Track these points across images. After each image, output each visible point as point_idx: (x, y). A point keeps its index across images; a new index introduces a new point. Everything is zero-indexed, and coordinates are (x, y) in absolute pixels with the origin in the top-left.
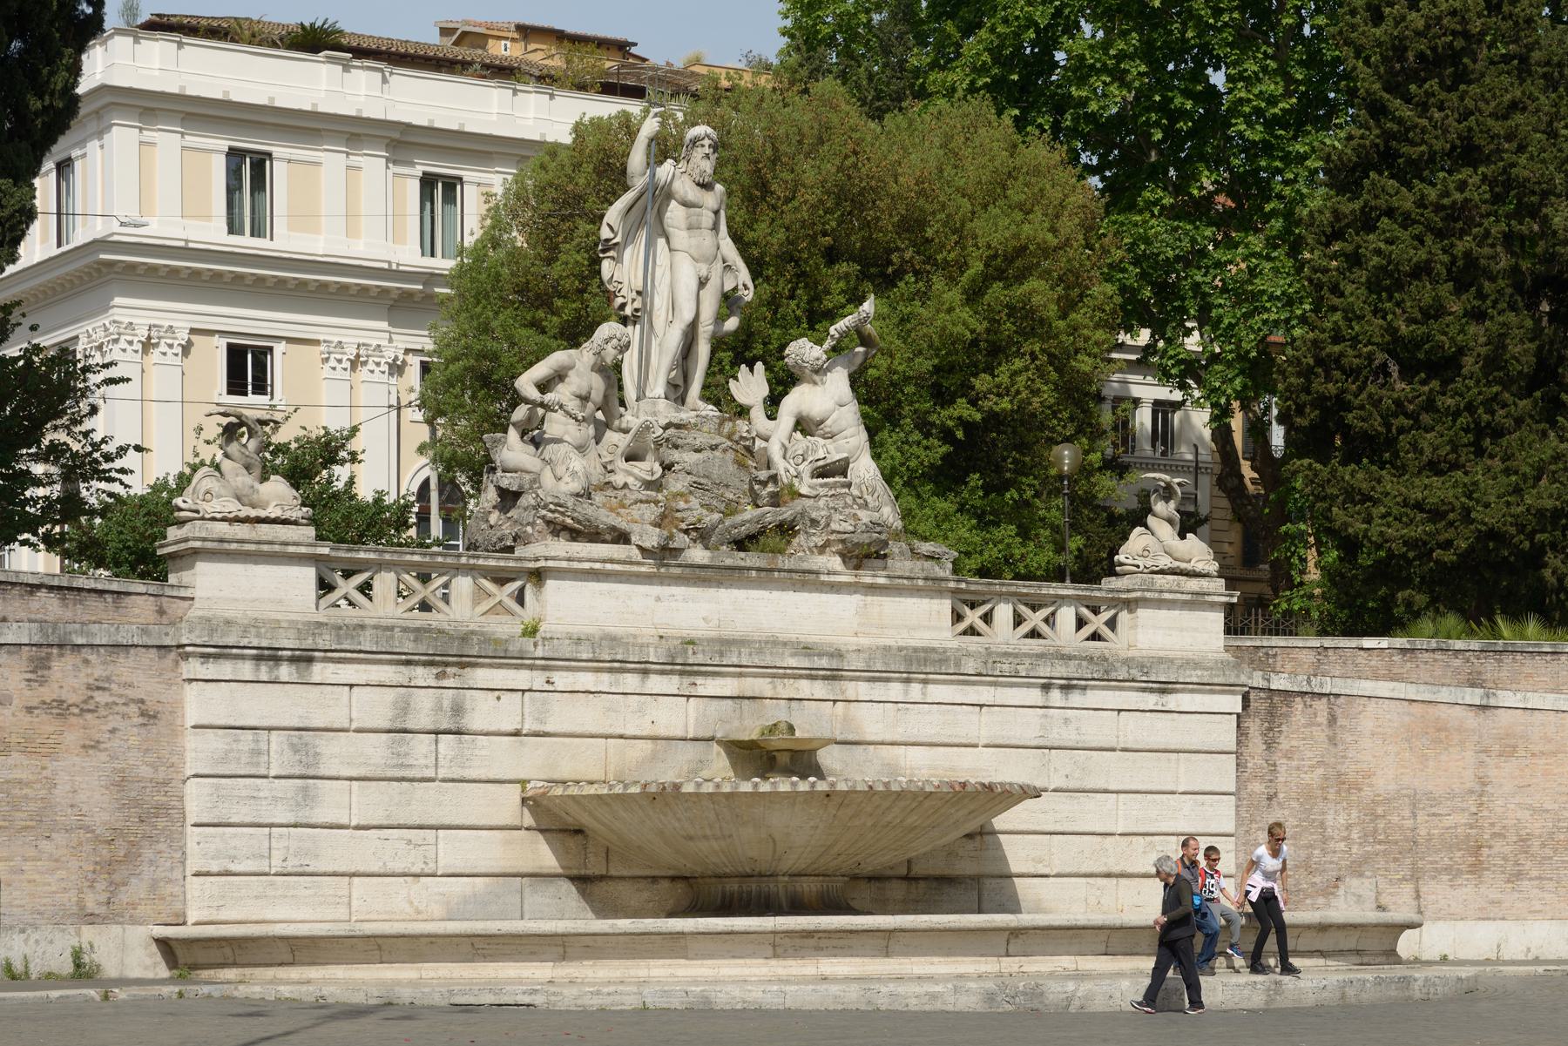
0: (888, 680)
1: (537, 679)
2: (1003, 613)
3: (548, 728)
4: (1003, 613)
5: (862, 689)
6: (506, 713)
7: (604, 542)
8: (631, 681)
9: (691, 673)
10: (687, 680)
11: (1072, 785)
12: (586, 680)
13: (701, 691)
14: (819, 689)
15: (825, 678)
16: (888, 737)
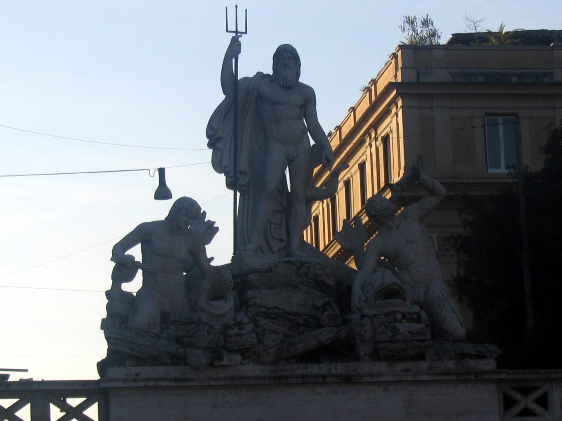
7: (164, 364)
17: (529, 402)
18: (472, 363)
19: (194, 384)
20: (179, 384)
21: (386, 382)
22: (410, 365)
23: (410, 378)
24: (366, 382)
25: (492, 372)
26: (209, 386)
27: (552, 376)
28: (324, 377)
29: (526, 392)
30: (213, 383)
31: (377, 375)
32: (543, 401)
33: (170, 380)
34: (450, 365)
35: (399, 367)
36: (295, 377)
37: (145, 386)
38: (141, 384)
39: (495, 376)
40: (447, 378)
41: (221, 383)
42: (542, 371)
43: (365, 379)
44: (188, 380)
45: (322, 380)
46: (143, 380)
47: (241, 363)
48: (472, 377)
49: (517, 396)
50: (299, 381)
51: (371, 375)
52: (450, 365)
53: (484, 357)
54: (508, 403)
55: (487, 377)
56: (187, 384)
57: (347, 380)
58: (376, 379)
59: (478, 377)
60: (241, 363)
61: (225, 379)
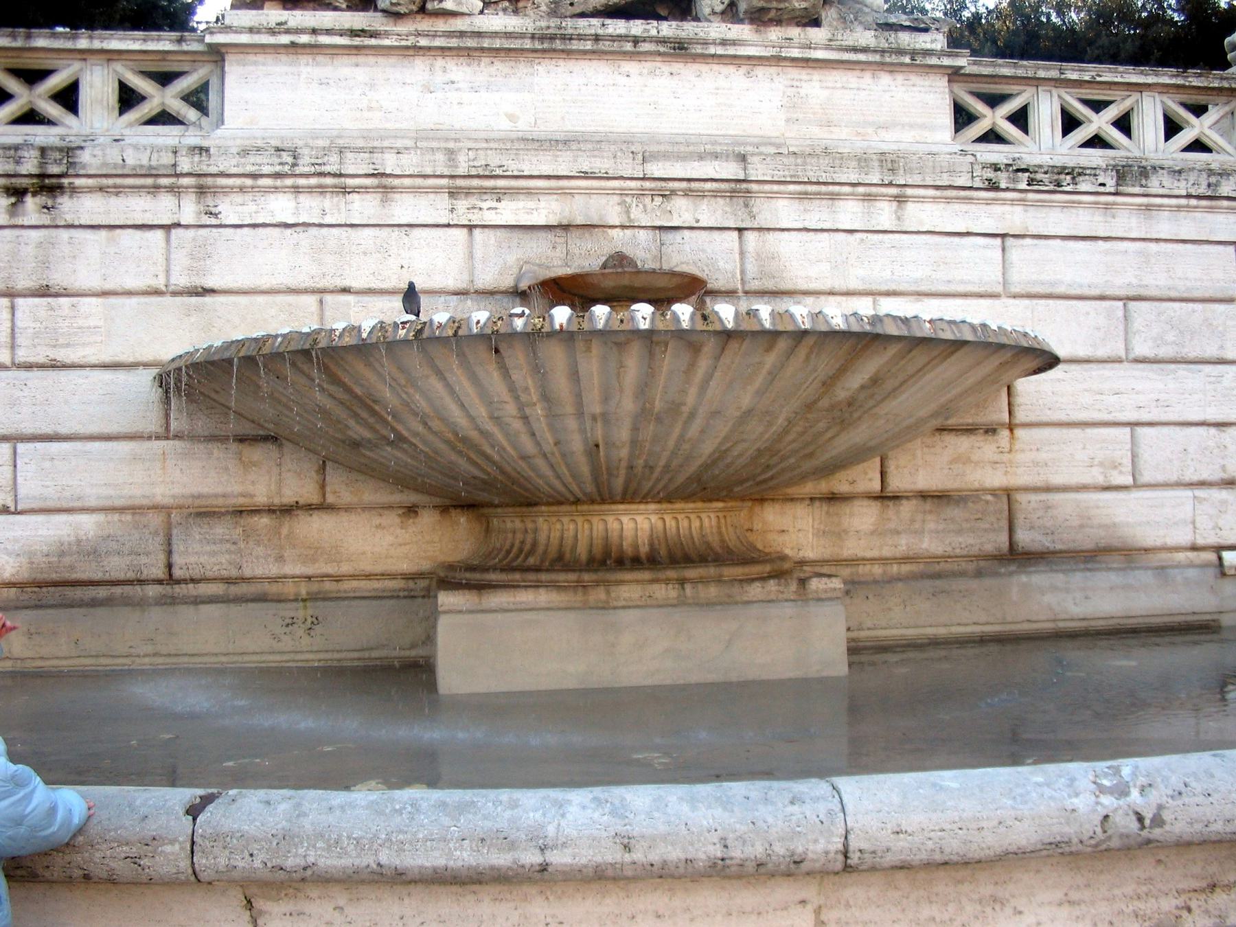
0: (833, 197)
1: (189, 210)
2: (1045, 112)
3: (210, 283)
4: (1045, 112)
5: (784, 211)
6: (140, 260)
8: (362, 207)
9: (468, 192)
10: (462, 204)
11: (1163, 352)
12: (281, 207)
13: (491, 218)
14: (709, 212)
15: (715, 194)
16: (839, 284)
17: (996, 118)
18: (905, 39)
19: (387, 42)
20: (357, 41)
21: (749, 58)
22: (794, 32)
23: (796, 53)
24: (713, 56)
25: (941, 54)
26: (417, 49)
27: (1042, 74)
28: (636, 41)
29: (994, 101)
30: (423, 42)
31: (734, 43)
32: (1020, 119)
33: (341, 33)
34: (866, 38)
35: (775, 34)
36: (581, 37)
37: (293, 45)
38: (285, 39)
39: (946, 61)
40: (862, 57)
41: (438, 42)
42: (1025, 63)
43: (712, 50)
44: (373, 34)
45: (634, 50)
46: (288, 31)
47: (482, 12)
48: (907, 60)
49: (979, 107)
50: (589, 45)
51: (724, 42)
52: (866, 38)
53: (926, 30)
54: (963, 117)
55: (934, 61)
56: (373, 42)
57: (680, 50)
58: (731, 51)
59: (917, 62)
60: (482, 12)
61: (449, 34)
